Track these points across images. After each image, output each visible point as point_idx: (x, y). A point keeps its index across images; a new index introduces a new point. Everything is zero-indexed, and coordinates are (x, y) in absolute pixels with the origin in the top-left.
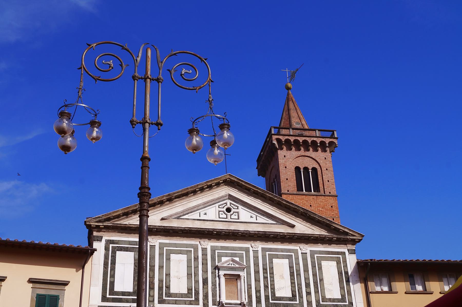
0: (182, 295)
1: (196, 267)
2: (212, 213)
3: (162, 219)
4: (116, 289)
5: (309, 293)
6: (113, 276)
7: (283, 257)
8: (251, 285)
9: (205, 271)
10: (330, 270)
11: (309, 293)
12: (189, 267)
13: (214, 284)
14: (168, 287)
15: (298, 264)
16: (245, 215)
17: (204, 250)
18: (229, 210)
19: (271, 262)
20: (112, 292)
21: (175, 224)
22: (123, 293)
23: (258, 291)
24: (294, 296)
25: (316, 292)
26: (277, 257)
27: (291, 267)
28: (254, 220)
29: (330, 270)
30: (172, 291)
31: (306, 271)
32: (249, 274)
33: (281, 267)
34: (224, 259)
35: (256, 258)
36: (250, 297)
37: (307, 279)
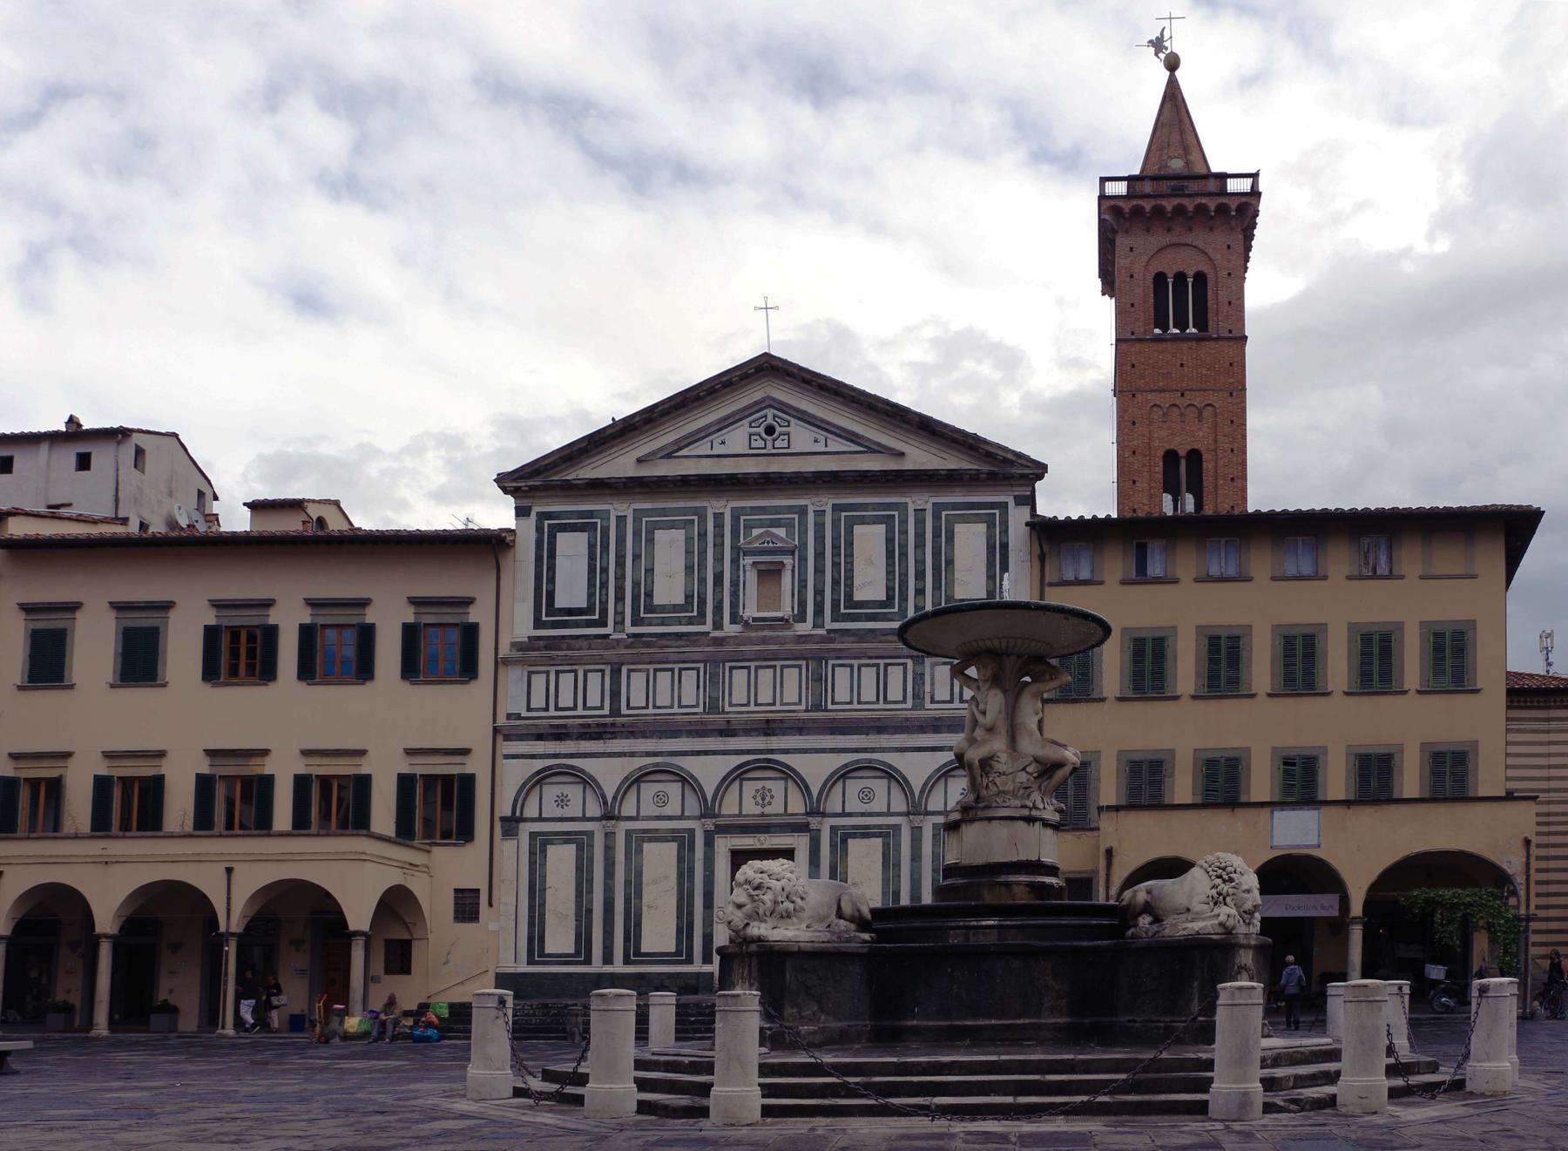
0: (675, 608)
1: (703, 553)
2: (737, 439)
3: (639, 461)
6: (551, 580)
7: (876, 521)
8: (806, 581)
9: (719, 559)
10: (970, 541)
12: (689, 552)
13: (735, 584)
14: (649, 595)
15: (904, 532)
16: (802, 438)
17: (719, 517)
18: (770, 430)
19: (850, 532)
20: (552, 610)
23: (819, 592)
24: (890, 597)
26: (863, 521)
27: (889, 541)
28: (820, 448)
29: (970, 541)
30: (658, 600)
31: (920, 545)
32: (803, 559)
33: (870, 541)
34: (756, 532)
35: (820, 527)
36: (802, 604)
37: (920, 562)
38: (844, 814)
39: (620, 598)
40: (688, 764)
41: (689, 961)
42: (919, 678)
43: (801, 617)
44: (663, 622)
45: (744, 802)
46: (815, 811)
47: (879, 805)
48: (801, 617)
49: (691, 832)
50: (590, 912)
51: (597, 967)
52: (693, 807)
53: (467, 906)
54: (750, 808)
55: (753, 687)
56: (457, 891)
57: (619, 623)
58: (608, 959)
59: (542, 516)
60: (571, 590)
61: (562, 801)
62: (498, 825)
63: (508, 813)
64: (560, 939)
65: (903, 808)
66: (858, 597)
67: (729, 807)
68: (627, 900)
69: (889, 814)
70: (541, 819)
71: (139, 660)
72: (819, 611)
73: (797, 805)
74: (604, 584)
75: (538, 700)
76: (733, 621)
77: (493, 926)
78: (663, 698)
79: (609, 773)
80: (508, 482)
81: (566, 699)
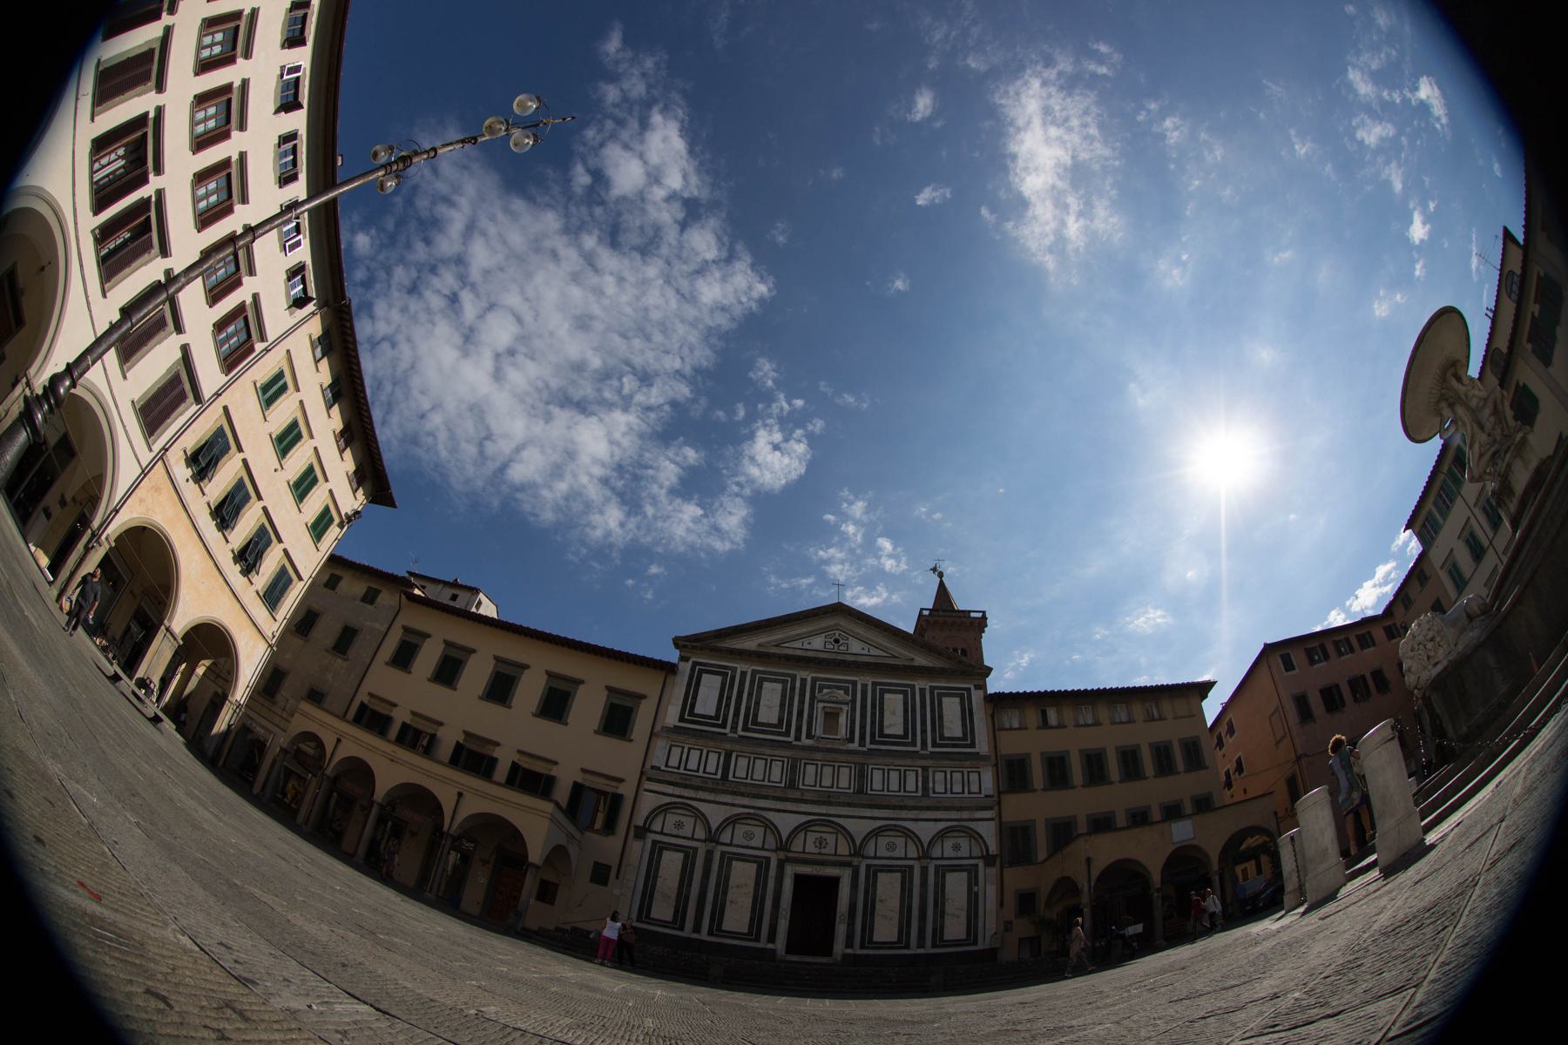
1: (791, 699)
4: (697, 711)
5: (924, 732)
6: (695, 698)
9: (802, 702)
10: (951, 707)
11: (924, 732)
14: (756, 715)
15: (914, 699)
17: (803, 681)
19: (882, 698)
20: (692, 713)
21: (774, 650)
22: (703, 716)
23: (863, 727)
25: (933, 730)
26: (890, 692)
29: (951, 707)
32: (853, 709)
33: (894, 702)
38: (875, 857)
39: (736, 714)
40: (770, 815)
41: (757, 939)
42: (925, 780)
43: (851, 740)
44: (763, 732)
45: (808, 844)
46: (858, 852)
47: (899, 853)
48: (851, 740)
49: (768, 859)
50: (687, 898)
51: (687, 932)
52: (771, 842)
53: (601, 874)
54: (810, 847)
55: (819, 776)
56: (596, 864)
57: (734, 729)
58: (697, 929)
59: (695, 664)
60: (707, 702)
61: (679, 825)
62: (632, 833)
63: (641, 823)
64: (663, 910)
65: (915, 855)
66: (887, 731)
67: (797, 846)
68: (716, 895)
69: (906, 858)
70: (662, 833)
71: (448, 672)
72: (862, 738)
73: (844, 849)
74: (728, 706)
75: (674, 762)
76: (809, 736)
77: (617, 892)
78: (758, 775)
79: (716, 815)
80: (679, 642)
81: (693, 765)
